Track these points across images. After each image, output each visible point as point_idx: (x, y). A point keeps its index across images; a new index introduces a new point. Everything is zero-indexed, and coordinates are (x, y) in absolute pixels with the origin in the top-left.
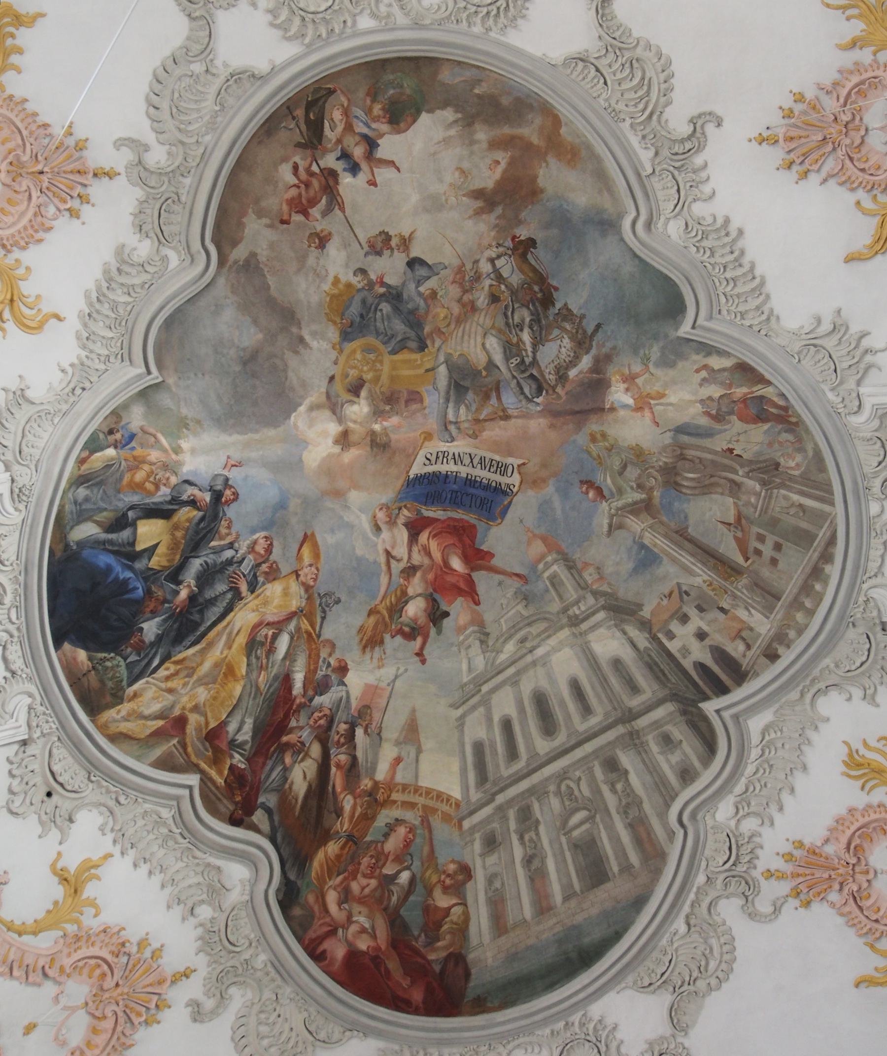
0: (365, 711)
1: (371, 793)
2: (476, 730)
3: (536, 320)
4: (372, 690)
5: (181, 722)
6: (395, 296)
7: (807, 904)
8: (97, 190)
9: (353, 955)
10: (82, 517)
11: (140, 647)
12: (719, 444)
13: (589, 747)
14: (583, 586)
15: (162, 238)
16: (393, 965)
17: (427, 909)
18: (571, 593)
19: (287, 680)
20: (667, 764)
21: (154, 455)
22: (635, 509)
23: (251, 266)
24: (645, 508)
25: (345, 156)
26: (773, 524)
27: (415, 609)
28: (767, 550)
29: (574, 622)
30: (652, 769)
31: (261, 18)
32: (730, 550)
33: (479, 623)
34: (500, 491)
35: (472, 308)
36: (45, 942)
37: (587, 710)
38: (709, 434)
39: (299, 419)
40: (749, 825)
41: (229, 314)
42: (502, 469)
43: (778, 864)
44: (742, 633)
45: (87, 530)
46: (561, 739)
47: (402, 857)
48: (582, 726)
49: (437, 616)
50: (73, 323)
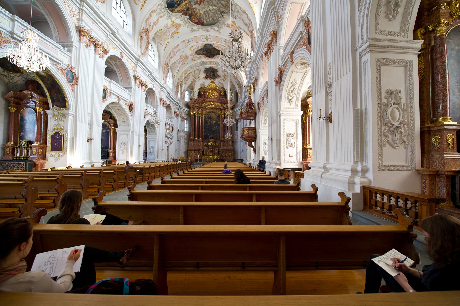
2: (204, 10)
5: (180, 10)
11: (175, 7)
19: (188, 7)
29: (212, 6)
32: (224, 5)
47: (199, 17)
49: (200, 3)
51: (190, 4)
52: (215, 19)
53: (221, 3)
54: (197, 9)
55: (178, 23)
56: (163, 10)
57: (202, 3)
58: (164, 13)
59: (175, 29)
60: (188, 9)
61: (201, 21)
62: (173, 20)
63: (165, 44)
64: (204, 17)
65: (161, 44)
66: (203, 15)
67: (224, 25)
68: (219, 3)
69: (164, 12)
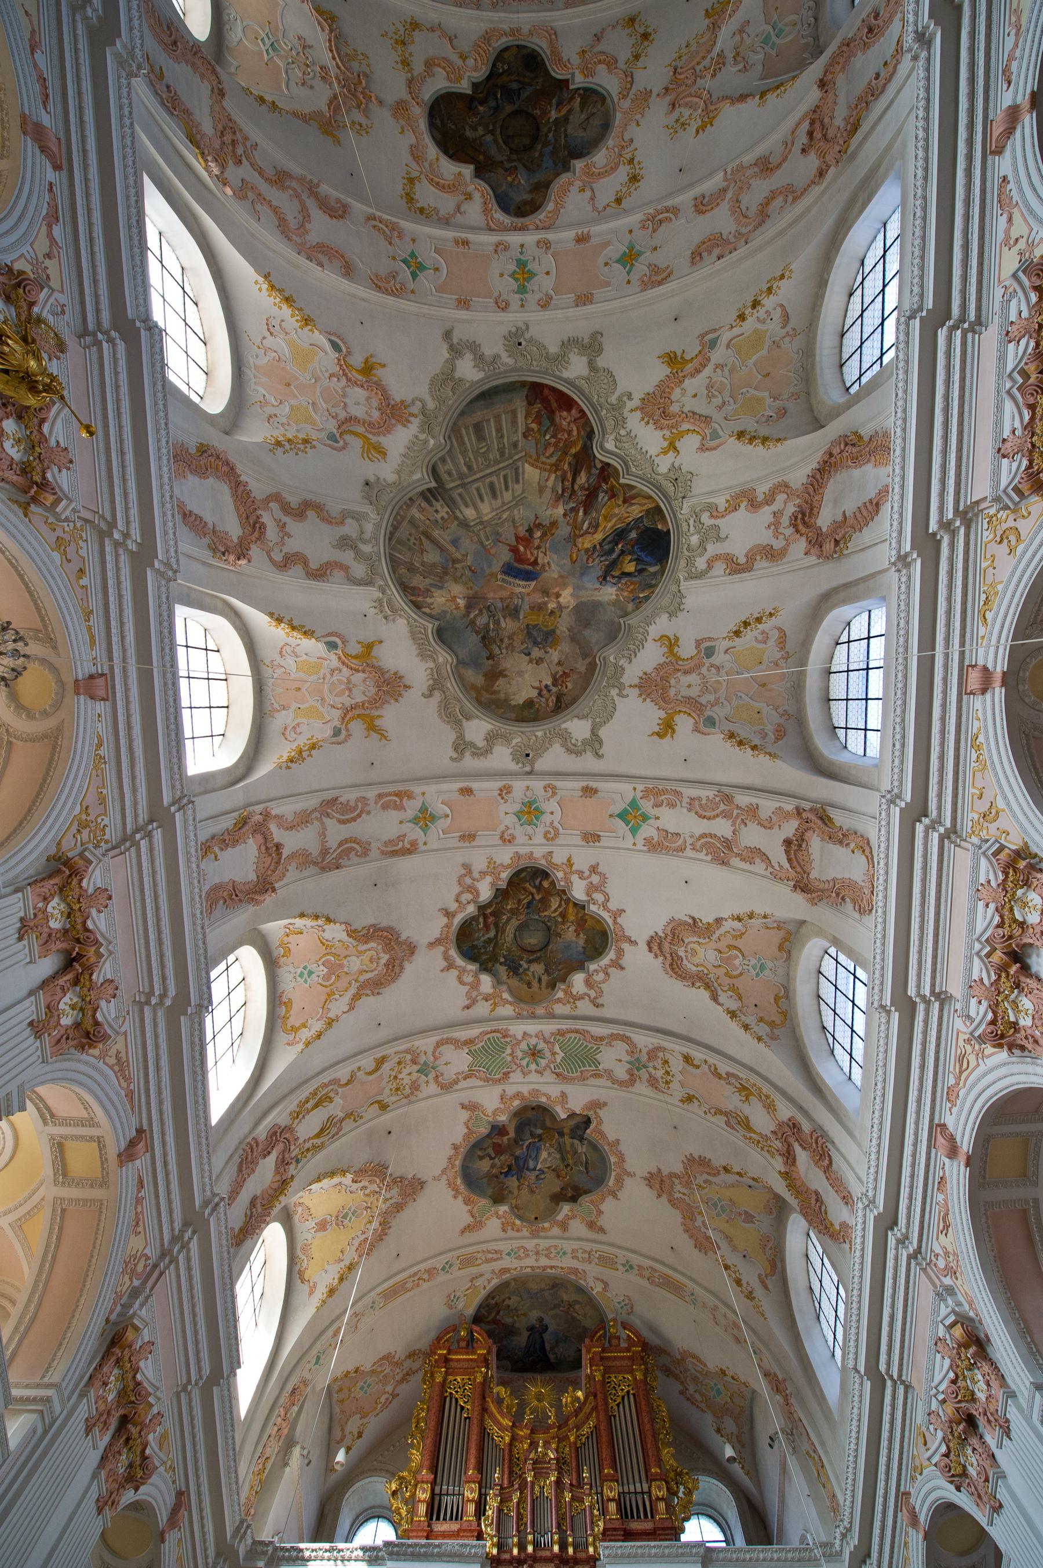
0: (558, 499)
1: (557, 470)
2: (518, 488)
3: (488, 632)
4: (555, 506)
5: (625, 501)
6: (536, 643)
7: (402, 402)
8: (637, 681)
9: (569, 410)
10: (655, 574)
12: (428, 581)
13: (478, 476)
14: (478, 535)
15: (616, 665)
16: (554, 405)
17: (540, 423)
18: (482, 533)
19: (585, 513)
20: (450, 465)
21: (626, 594)
22: (458, 561)
23: (585, 656)
24: (455, 561)
25: (549, 691)
26: (410, 549)
27: (538, 534)
28: (412, 540)
29: (481, 523)
30: (455, 464)
31: (574, 735)
33: (515, 527)
34: (505, 573)
35: (510, 638)
36: (685, 426)
37: (478, 490)
38: (432, 585)
39: (573, 603)
40: (423, 437)
41: (594, 640)
42: (503, 581)
43: (412, 419)
44: (422, 510)
45: (652, 569)
46: (488, 480)
47: (547, 445)
48: (479, 484)
49: (530, 531)
50: (650, 639)
51: (576, 526)
52: (470, 439)
53: (442, 549)
54: (548, 494)
55: (651, 426)
56: (694, 540)
57: (522, 532)
58: (691, 522)
59: (676, 394)
60: (590, 500)
61: (538, 419)
62: (671, 454)
63: (761, 312)
64: (522, 442)
65: (786, 317)
66: (526, 458)
67: (423, 411)
68: (450, 547)
69: (692, 528)
